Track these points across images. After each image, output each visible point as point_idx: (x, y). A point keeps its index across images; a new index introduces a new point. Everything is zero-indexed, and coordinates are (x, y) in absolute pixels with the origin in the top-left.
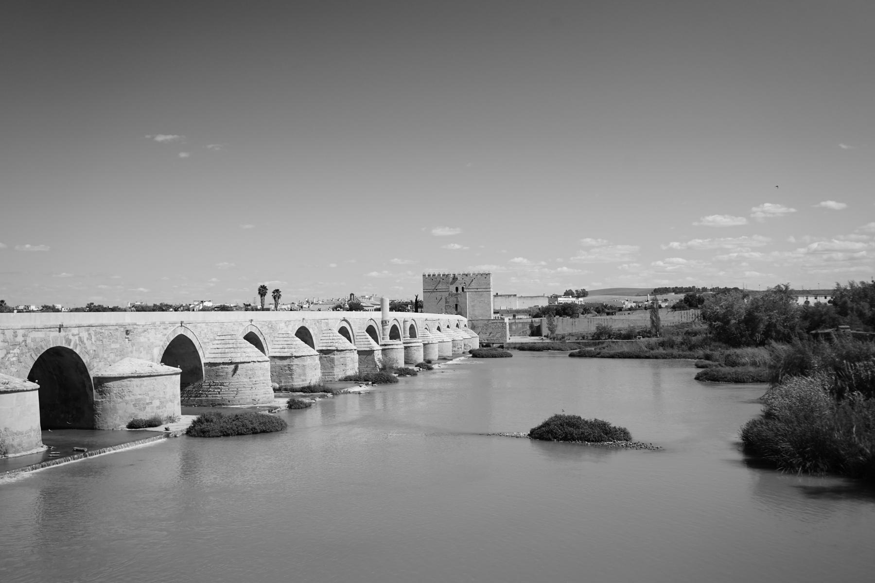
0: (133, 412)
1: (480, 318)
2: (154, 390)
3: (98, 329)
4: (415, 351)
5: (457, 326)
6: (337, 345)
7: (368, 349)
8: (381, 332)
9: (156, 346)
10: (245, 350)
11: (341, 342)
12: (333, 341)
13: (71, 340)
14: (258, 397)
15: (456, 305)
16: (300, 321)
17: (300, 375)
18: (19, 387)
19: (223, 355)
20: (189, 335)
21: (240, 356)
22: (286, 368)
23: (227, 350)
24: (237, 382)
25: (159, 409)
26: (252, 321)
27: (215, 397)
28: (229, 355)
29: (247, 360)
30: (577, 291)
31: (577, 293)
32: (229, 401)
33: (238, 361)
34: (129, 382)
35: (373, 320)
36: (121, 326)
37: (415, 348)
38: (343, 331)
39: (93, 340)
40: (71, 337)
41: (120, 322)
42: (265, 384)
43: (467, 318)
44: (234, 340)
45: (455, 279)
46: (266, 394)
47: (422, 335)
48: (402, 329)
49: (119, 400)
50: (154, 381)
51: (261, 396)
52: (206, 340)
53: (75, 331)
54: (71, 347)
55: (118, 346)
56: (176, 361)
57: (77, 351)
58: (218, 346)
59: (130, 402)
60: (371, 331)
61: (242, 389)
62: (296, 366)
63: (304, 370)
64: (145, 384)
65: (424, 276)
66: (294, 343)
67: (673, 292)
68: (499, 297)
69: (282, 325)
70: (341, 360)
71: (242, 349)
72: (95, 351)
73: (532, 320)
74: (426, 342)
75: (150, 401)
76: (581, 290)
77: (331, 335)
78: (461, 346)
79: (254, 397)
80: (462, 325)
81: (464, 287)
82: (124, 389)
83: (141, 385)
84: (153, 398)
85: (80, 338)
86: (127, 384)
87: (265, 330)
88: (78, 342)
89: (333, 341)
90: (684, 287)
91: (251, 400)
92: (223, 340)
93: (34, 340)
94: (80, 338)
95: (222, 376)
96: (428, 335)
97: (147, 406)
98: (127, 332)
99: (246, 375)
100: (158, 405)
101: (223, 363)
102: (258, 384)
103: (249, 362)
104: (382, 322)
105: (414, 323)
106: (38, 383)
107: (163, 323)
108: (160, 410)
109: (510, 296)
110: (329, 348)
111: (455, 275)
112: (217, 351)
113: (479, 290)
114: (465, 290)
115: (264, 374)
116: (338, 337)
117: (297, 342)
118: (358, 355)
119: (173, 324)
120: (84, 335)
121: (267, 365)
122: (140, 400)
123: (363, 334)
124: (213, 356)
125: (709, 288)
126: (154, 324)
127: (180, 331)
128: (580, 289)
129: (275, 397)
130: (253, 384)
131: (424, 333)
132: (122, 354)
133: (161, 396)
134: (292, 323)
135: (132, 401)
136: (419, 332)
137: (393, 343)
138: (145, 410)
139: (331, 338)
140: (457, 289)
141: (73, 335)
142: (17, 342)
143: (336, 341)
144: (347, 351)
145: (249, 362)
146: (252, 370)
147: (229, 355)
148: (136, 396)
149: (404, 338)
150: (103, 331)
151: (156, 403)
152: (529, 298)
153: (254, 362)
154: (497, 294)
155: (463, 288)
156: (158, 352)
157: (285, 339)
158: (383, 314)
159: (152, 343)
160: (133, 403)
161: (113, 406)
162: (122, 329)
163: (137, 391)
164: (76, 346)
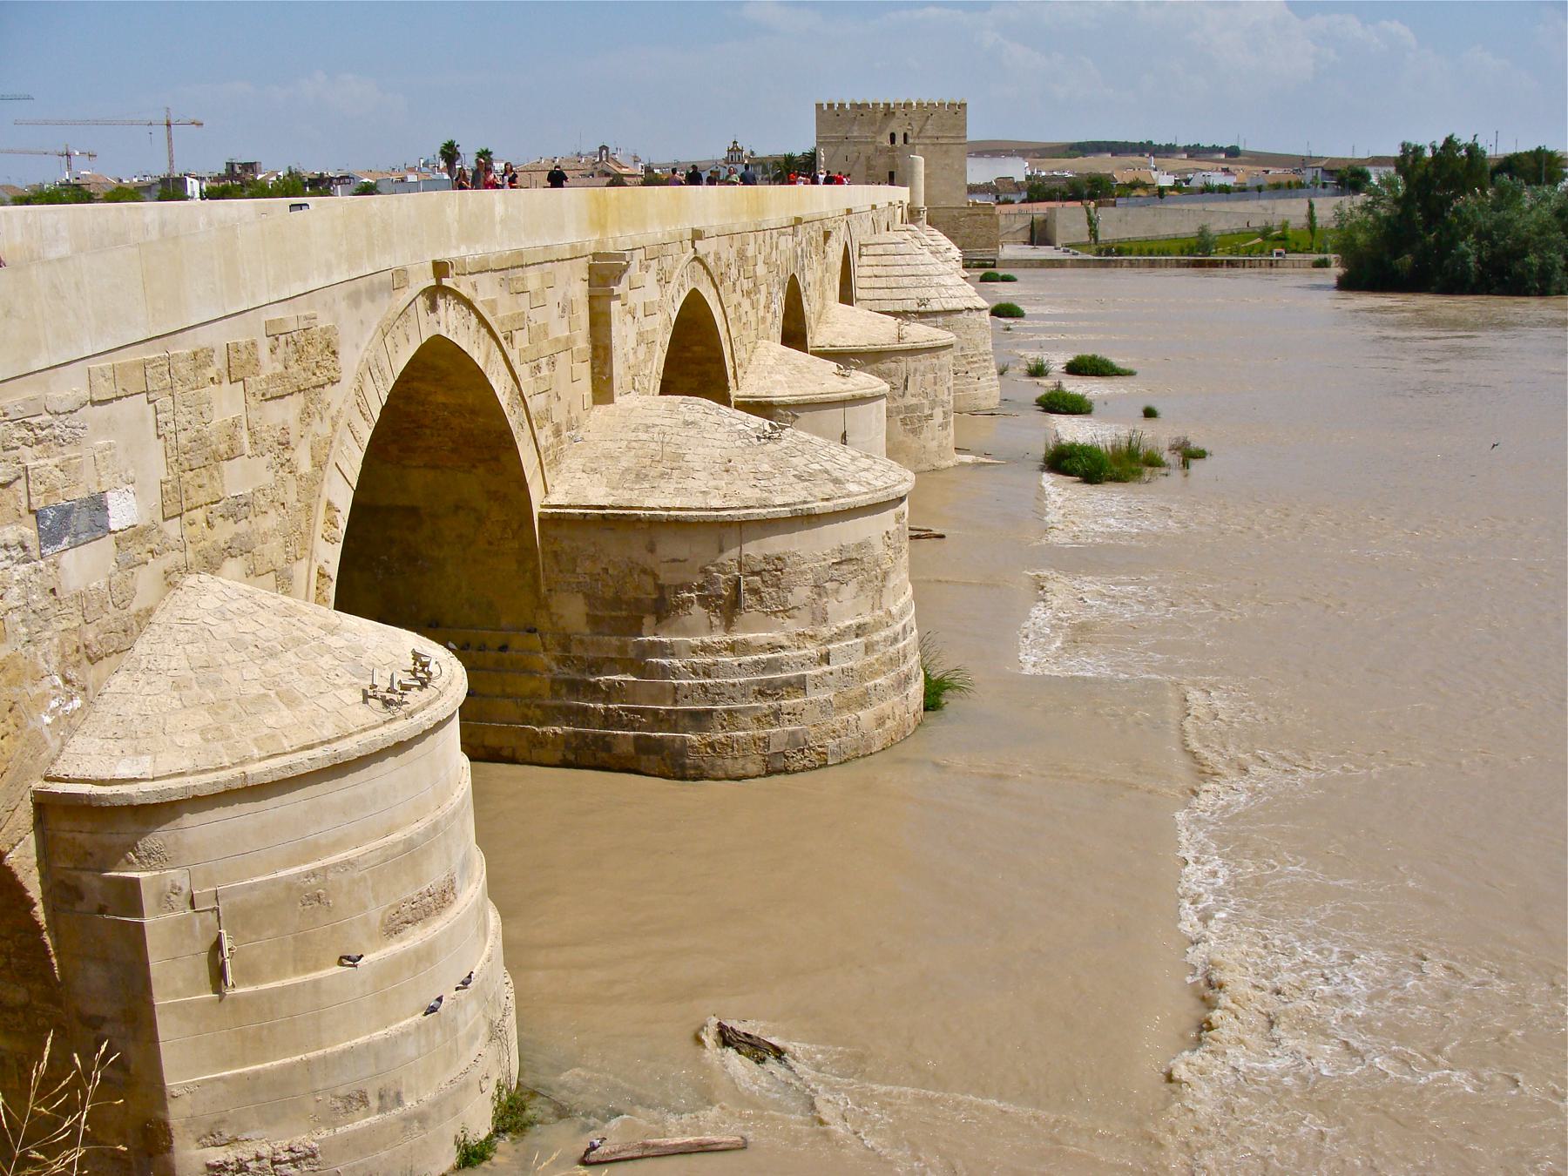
28: (914, 293)
34: (893, 365)
45: (889, 112)
50: (935, 361)
59: (894, 414)
65: (819, 106)
71: (936, 280)
81: (909, 133)
83: (916, 370)
103: (960, 311)
111: (889, 105)
113: (940, 141)
114: (910, 141)
125: (1181, 144)
135: (898, 413)
147: (914, 293)
160: (902, 417)
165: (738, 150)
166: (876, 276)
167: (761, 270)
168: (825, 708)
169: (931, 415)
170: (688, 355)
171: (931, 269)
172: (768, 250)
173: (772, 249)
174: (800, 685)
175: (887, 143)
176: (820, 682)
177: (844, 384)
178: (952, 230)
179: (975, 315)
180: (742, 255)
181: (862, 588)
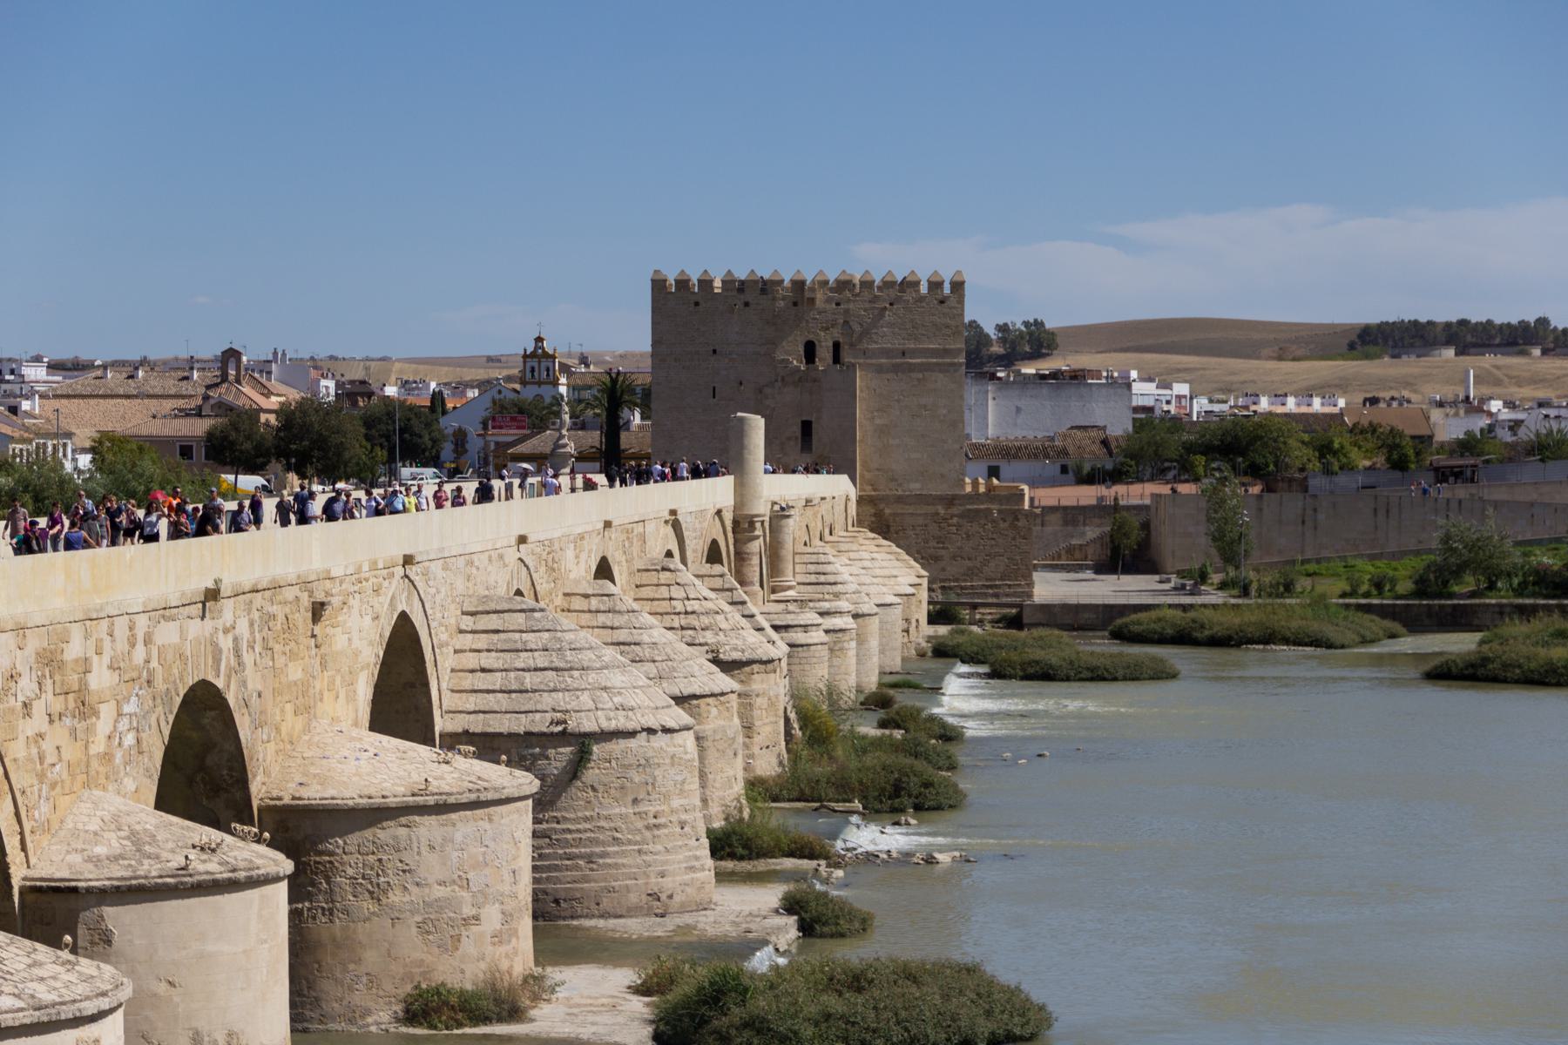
0: (417, 955)
1: (915, 487)
2: (487, 864)
6: (709, 637)
9: (362, 669)
11: (724, 625)
12: (692, 620)
14: (668, 883)
15: (807, 427)
19: (519, 702)
21: (591, 705)
23: (529, 680)
24: (586, 819)
26: (522, 540)
28: (547, 700)
29: (620, 722)
30: (1003, 328)
31: (1003, 341)
32: (557, 901)
33: (588, 725)
34: (402, 832)
39: (258, 649)
44: (546, 635)
46: (692, 869)
47: (813, 578)
49: (368, 906)
50: (486, 825)
51: (678, 878)
54: (220, 684)
58: (488, 660)
61: (610, 849)
64: (458, 837)
66: (646, 638)
67: (1448, 343)
71: (592, 677)
75: (474, 912)
76: (1026, 324)
77: (677, 592)
79: (654, 883)
82: (385, 858)
85: (236, 639)
86: (395, 838)
89: (692, 620)
90: (1498, 321)
91: (644, 897)
92: (497, 631)
96: (839, 579)
97: (464, 933)
98: (318, 610)
100: (499, 927)
101: (529, 734)
102: (665, 826)
103: (632, 734)
104: (736, 523)
108: (502, 950)
112: (482, 681)
114: (847, 357)
115: (683, 782)
116: (709, 605)
122: (439, 905)
124: (471, 702)
130: (648, 828)
131: (821, 568)
133: (506, 888)
138: (457, 949)
139: (679, 606)
140: (810, 352)
141: (226, 631)
143: (705, 620)
144: (756, 667)
145: (632, 734)
147: (547, 700)
148: (427, 890)
151: (492, 917)
153: (650, 731)
155: (837, 346)
159: (356, 654)
160: (419, 918)
163: (431, 867)
165: (546, 355)
166: (483, 670)
167: (101, 679)
169: (476, 917)
171: (587, 657)
172: (122, 645)
173: (133, 645)
175: (799, 363)
177: (204, 861)
178: (933, 543)
179: (660, 740)
180: (50, 661)
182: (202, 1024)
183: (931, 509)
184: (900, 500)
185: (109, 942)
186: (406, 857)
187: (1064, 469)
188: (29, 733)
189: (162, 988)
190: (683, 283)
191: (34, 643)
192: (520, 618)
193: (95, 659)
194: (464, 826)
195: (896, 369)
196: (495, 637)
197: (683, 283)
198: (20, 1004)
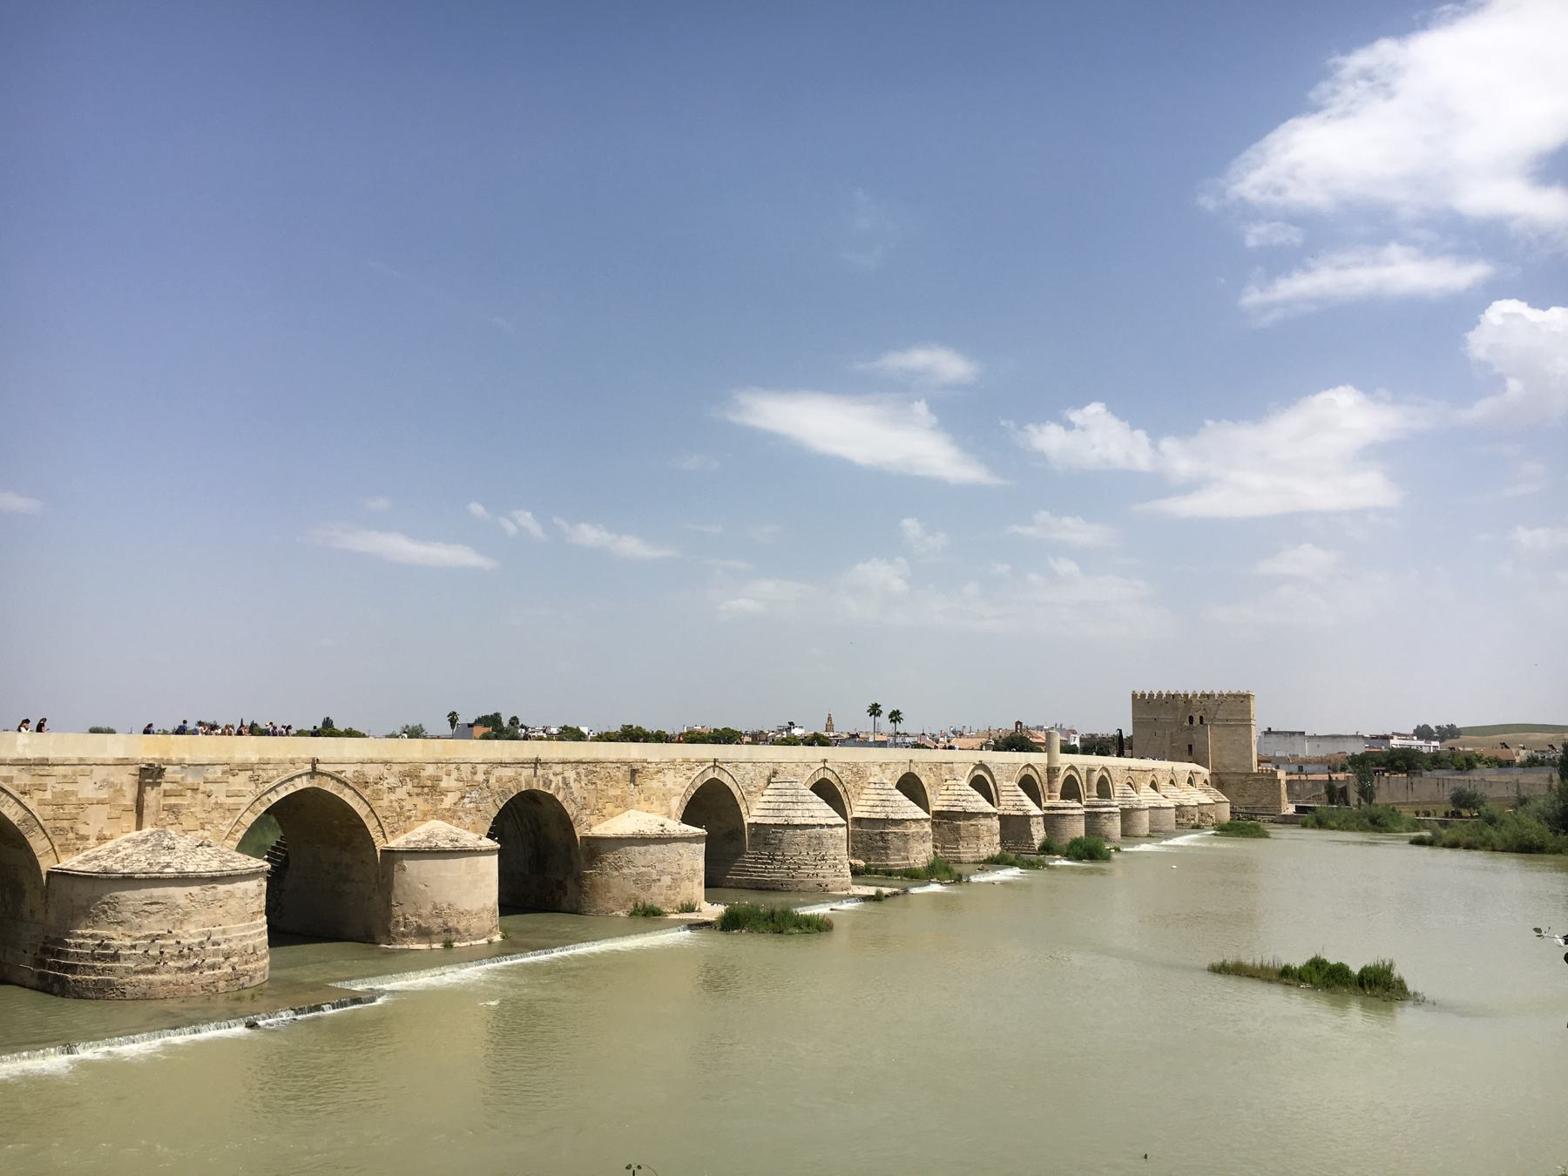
1: (1233, 770)
3: (591, 767)
4: (1106, 821)
5: (1190, 782)
6: (964, 804)
7: (1021, 813)
8: (1046, 786)
10: (809, 806)
13: (551, 781)
15: (1190, 746)
16: (904, 763)
17: (899, 850)
18: (470, 845)
20: (727, 780)
22: (878, 838)
23: (782, 806)
25: (671, 889)
26: (825, 761)
27: (762, 876)
29: (810, 821)
30: (1438, 727)
31: (1438, 732)
32: (782, 885)
35: (1033, 767)
36: (624, 763)
37: (1107, 815)
38: (979, 784)
40: (551, 777)
41: (624, 757)
42: (837, 862)
43: (1208, 768)
48: (1085, 783)
52: (752, 789)
53: (558, 768)
54: (550, 792)
55: (619, 792)
56: (709, 818)
57: (560, 798)
58: (771, 799)
60: (1028, 785)
62: (893, 835)
63: (906, 842)
64: (651, 850)
65: (1134, 696)
68: (1273, 735)
69: (876, 769)
70: (972, 828)
71: (805, 806)
72: (584, 798)
73: (1330, 777)
74: (1127, 807)
75: (658, 877)
77: (957, 788)
78: (1194, 816)
80: (1199, 781)
84: (661, 873)
85: (564, 779)
87: (846, 776)
88: (561, 785)
89: (959, 797)
93: (499, 780)
94: (564, 779)
95: (773, 844)
98: (634, 772)
99: (809, 845)
101: (775, 824)
104: (1048, 770)
105: (1105, 774)
106: (497, 841)
107: (687, 761)
108: (672, 892)
109: (1293, 733)
110: (952, 809)
114: (1205, 722)
115: (836, 844)
116: (968, 792)
117: (897, 798)
118: (998, 822)
119: (701, 762)
120: (571, 774)
121: (842, 831)
123: (1012, 788)
126: (673, 762)
127: (711, 775)
128: (1444, 724)
129: (853, 884)
132: (623, 804)
133: (674, 870)
134: (892, 767)
136: (1117, 789)
137: (1066, 805)
139: (956, 793)
141: (556, 774)
142: (477, 781)
146: (818, 838)
147: (786, 812)
149: (1088, 797)
150: (598, 769)
151: (666, 880)
152: (1329, 739)
154: (1270, 729)
155: (1201, 718)
156: (677, 804)
157: (878, 791)
158: (1049, 756)
159: (670, 790)
161: (606, 880)
162: (626, 768)
163: (639, 861)
164: (558, 789)
168: (128, 970)
169: (659, 880)
170: (352, 823)
174: (115, 957)
176: (127, 958)
179: (826, 830)
181: (165, 916)
182: (438, 901)
183: (1239, 778)
184: (1227, 774)
185: (405, 870)
186: (629, 856)
187: (1329, 768)
188: (393, 798)
189: (422, 887)
190: (1143, 695)
191: (396, 768)
192: (787, 784)
193: (445, 777)
194: (653, 848)
195: (1224, 726)
196: (777, 791)
197: (1143, 695)
198: (174, 871)
